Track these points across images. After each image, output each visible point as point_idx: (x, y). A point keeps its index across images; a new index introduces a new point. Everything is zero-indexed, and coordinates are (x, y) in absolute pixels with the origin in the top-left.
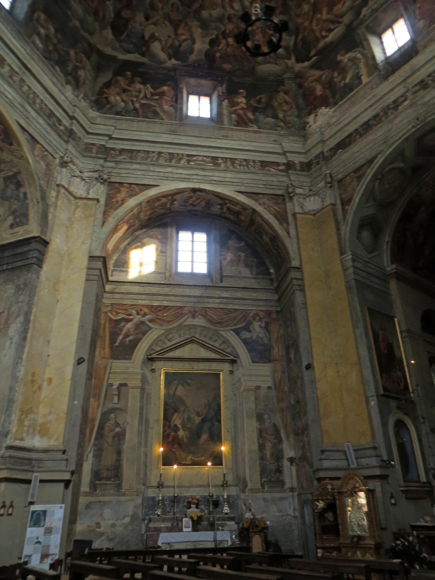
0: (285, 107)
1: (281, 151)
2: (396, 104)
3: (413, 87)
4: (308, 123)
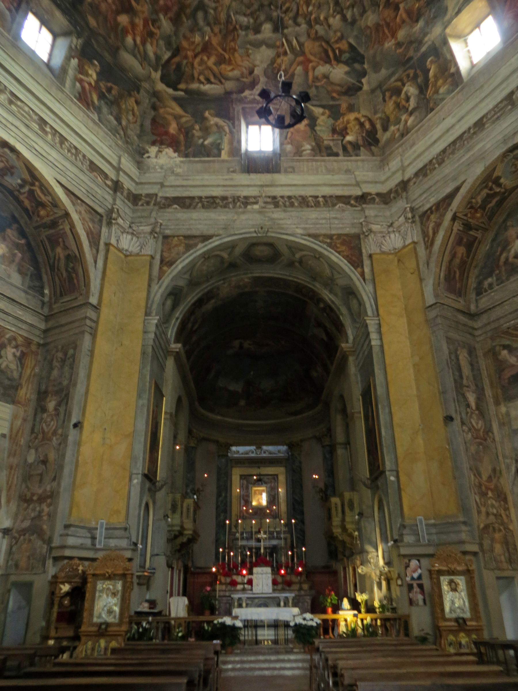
0: (131, 118)
1: (115, 163)
2: (246, 201)
3: (266, 197)
4: (148, 152)
